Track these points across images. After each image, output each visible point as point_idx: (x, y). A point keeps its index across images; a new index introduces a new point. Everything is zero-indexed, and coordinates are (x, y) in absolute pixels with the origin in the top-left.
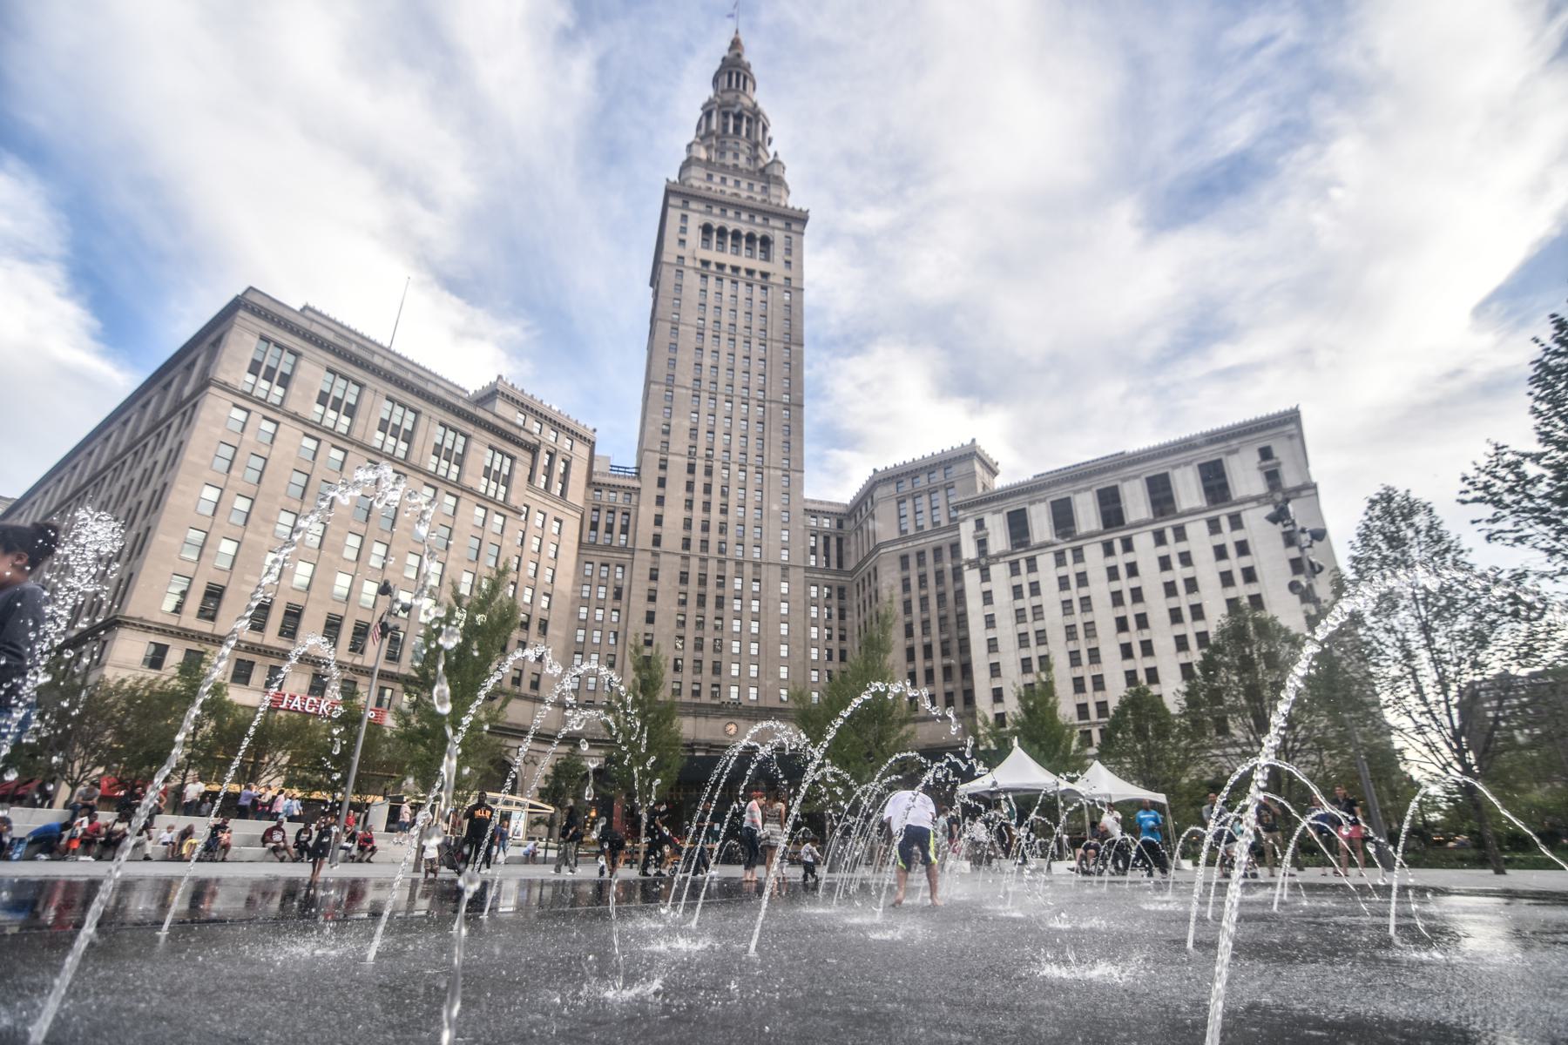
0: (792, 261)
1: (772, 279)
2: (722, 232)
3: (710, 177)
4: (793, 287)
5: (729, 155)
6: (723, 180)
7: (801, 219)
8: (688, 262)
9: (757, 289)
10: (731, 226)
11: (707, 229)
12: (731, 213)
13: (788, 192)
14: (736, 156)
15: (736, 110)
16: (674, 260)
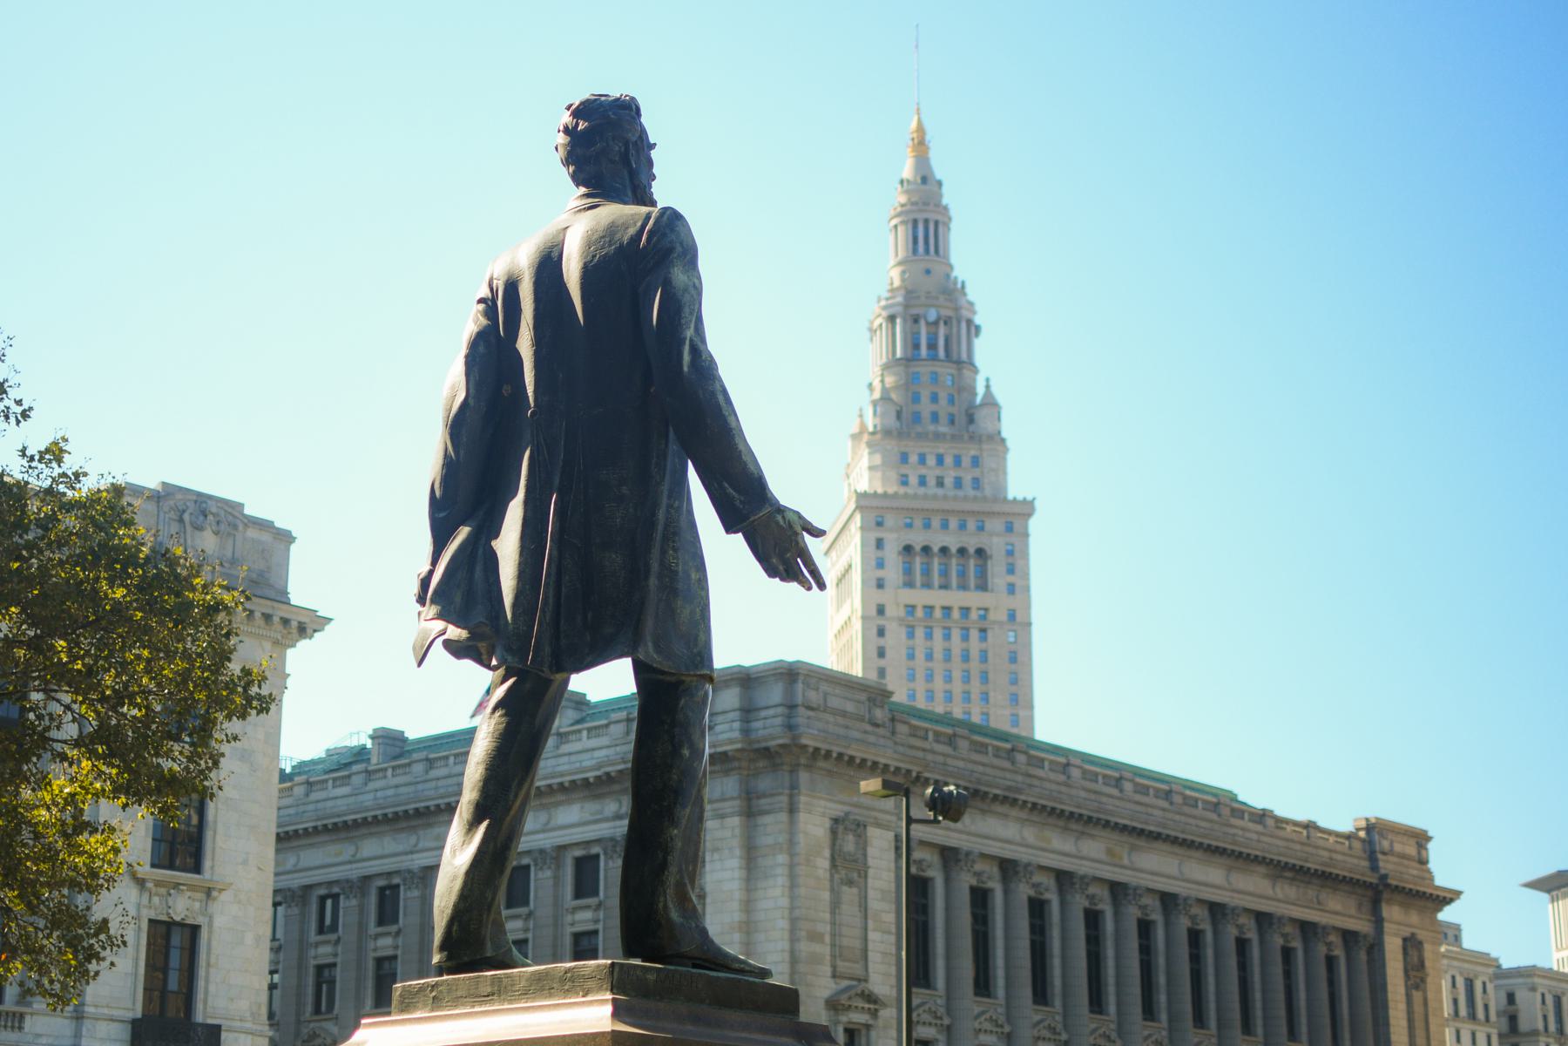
0: (1018, 588)
1: (992, 616)
2: (926, 550)
3: (904, 458)
4: (1019, 621)
5: (925, 395)
6: (922, 459)
7: (1026, 509)
8: (889, 612)
9: (974, 634)
10: (937, 540)
11: (908, 549)
12: (936, 523)
13: (1006, 450)
14: (934, 398)
15: (932, 315)
16: (874, 612)
